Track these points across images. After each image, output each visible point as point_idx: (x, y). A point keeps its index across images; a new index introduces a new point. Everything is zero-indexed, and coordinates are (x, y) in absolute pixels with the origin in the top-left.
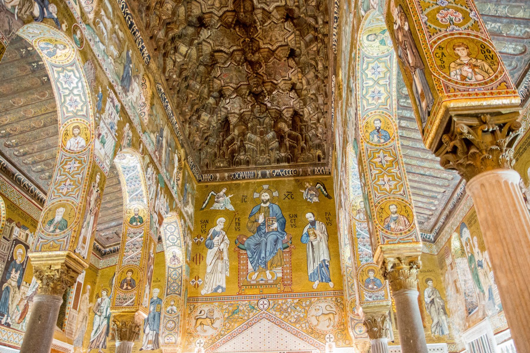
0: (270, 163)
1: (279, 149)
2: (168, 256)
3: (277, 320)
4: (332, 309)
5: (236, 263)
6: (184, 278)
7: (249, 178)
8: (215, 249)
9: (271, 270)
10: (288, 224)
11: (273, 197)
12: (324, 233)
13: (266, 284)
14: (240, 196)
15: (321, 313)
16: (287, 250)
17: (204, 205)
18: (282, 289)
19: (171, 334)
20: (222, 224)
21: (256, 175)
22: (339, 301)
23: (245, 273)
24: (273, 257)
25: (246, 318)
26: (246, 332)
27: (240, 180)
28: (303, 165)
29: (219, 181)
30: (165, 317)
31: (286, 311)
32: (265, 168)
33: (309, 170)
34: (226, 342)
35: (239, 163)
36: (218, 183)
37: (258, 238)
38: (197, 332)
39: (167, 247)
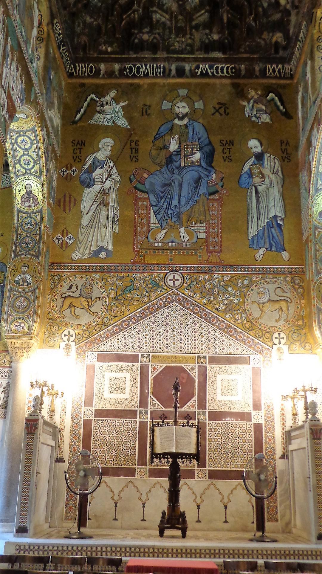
0: (192, 52)
1: (208, 25)
2: (19, 192)
4: (285, 295)
5: (130, 213)
6: (44, 229)
8: (97, 188)
9: (188, 227)
10: (218, 156)
11: (194, 111)
12: (277, 173)
13: (180, 249)
14: (140, 104)
15: (267, 299)
16: (216, 197)
17: (78, 116)
18: (206, 257)
19: (22, 318)
22: (297, 282)
23: (144, 229)
24: (192, 207)
26: (144, 322)
27: (140, 77)
29: (104, 77)
30: (12, 290)
31: (210, 292)
32: (184, 60)
33: (257, 68)
34: (112, 335)
35: (141, 47)
36: (102, 82)
37: (167, 174)
38: (65, 317)
39: (17, 177)
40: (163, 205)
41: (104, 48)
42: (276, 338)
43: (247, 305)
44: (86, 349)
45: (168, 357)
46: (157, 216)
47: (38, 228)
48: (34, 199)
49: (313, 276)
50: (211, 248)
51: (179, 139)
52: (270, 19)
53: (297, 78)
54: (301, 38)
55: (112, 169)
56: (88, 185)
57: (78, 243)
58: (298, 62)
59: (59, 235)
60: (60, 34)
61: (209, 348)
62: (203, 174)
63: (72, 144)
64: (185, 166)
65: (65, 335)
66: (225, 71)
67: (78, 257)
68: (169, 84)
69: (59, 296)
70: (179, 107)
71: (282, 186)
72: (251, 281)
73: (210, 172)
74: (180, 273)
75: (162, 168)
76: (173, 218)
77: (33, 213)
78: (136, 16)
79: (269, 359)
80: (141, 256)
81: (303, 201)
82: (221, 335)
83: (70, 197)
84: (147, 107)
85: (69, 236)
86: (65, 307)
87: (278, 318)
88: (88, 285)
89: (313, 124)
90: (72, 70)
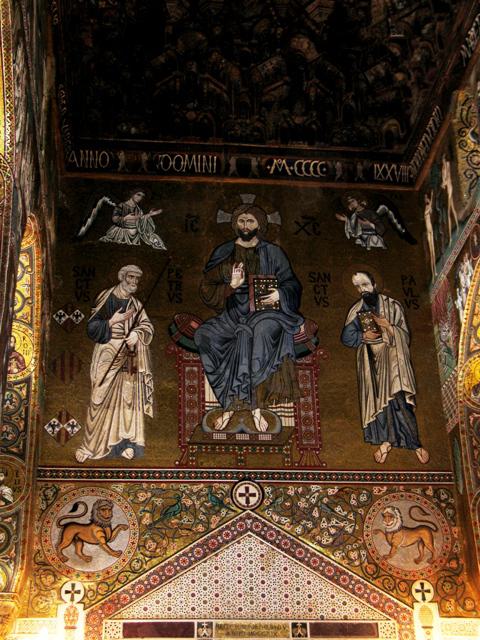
1: (287, 103)
3: (284, 537)
4: (426, 518)
7: (207, 174)
8: (116, 343)
10: (306, 297)
13: (254, 442)
15: (398, 525)
17: (83, 229)
18: (296, 458)
20: (133, 281)
21: (223, 167)
22: (443, 497)
23: (196, 411)
25: (201, 528)
26: (201, 566)
27: (181, 174)
28: (344, 154)
29: (123, 172)
31: (307, 514)
32: (249, 150)
33: (360, 167)
34: (147, 590)
36: (121, 178)
37: (229, 324)
38: (65, 560)
40: (224, 372)
41: (125, 128)
42: (417, 591)
43: (367, 536)
44: (103, 616)
45: (244, 626)
46: (217, 390)
47: (23, 409)
48: (19, 361)
49: (470, 489)
50: (305, 443)
51: (245, 268)
52: (378, 99)
53: (421, 183)
54: (430, 128)
55: (140, 313)
56: (101, 339)
57: (87, 433)
58: (423, 164)
59: (54, 419)
60: (63, 106)
61: (310, 610)
62: (286, 324)
63: (72, 273)
64: (257, 311)
65: (67, 592)
66: (311, 169)
67: (86, 457)
68: (226, 186)
69: (55, 523)
70: (243, 221)
71: (409, 346)
72: (370, 495)
73: (297, 321)
74: (258, 483)
75: (220, 314)
76: (241, 393)
77: (16, 383)
78: (178, 84)
79: (408, 627)
80: (193, 455)
81: (443, 369)
82: (329, 587)
83: (72, 358)
84: (193, 219)
85: (70, 422)
86: (66, 541)
87: (417, 557)
88: (104, 503)
89: (461, 254)
90: (73, 158)
